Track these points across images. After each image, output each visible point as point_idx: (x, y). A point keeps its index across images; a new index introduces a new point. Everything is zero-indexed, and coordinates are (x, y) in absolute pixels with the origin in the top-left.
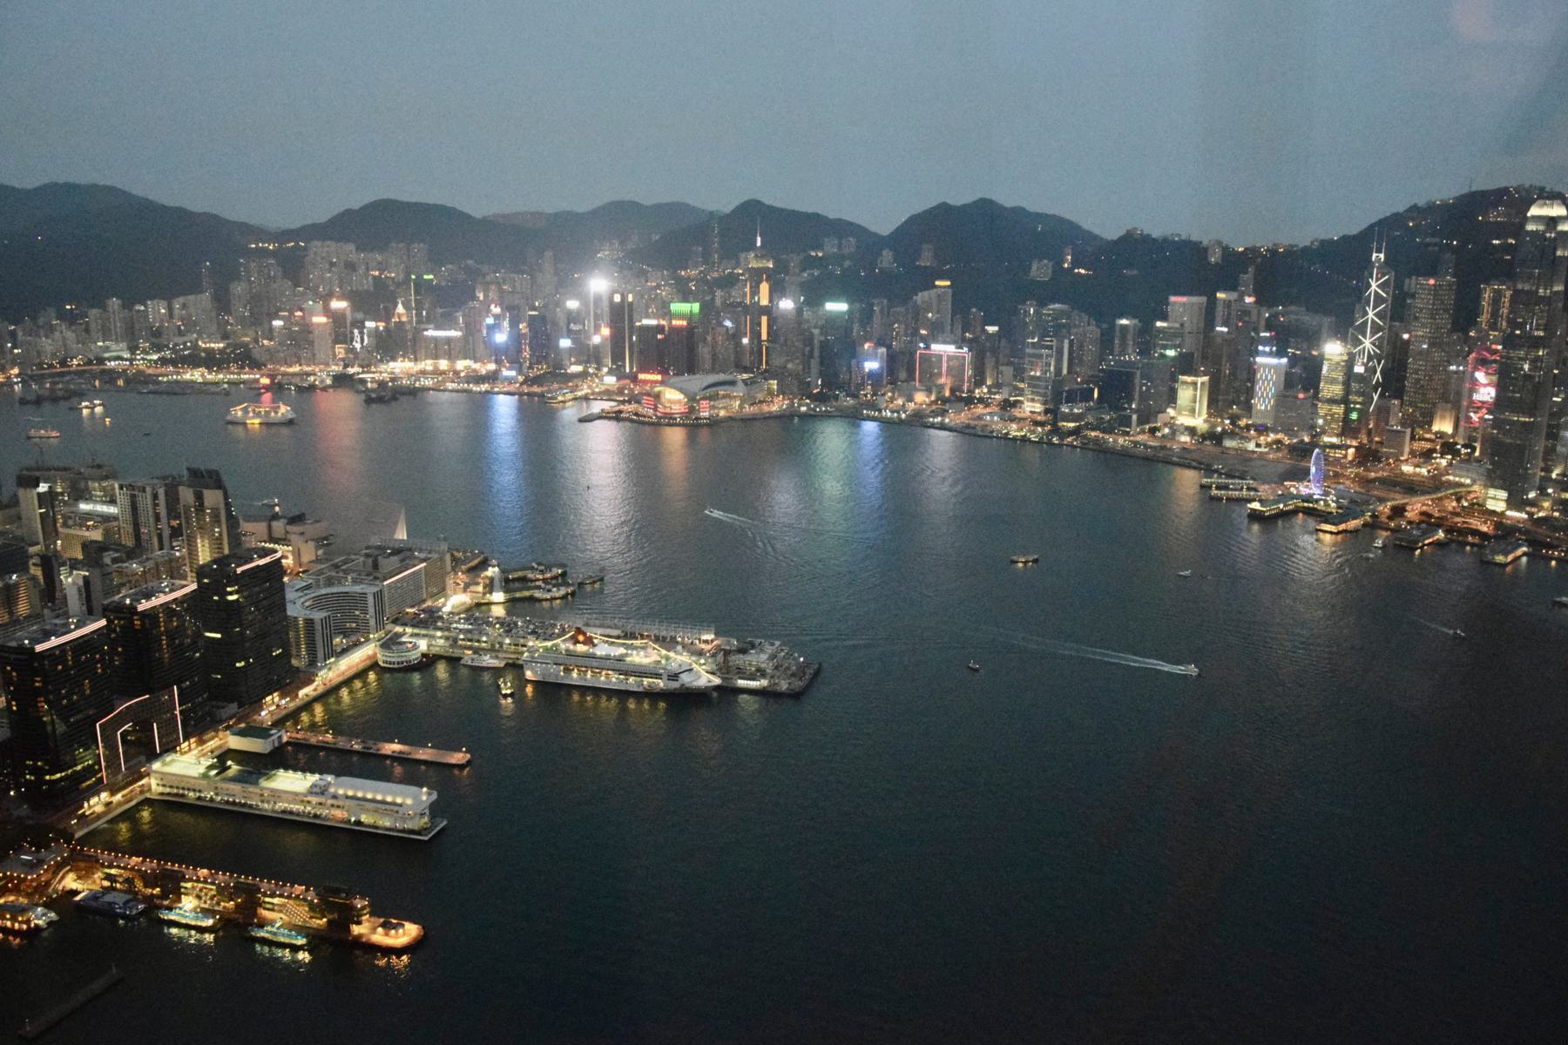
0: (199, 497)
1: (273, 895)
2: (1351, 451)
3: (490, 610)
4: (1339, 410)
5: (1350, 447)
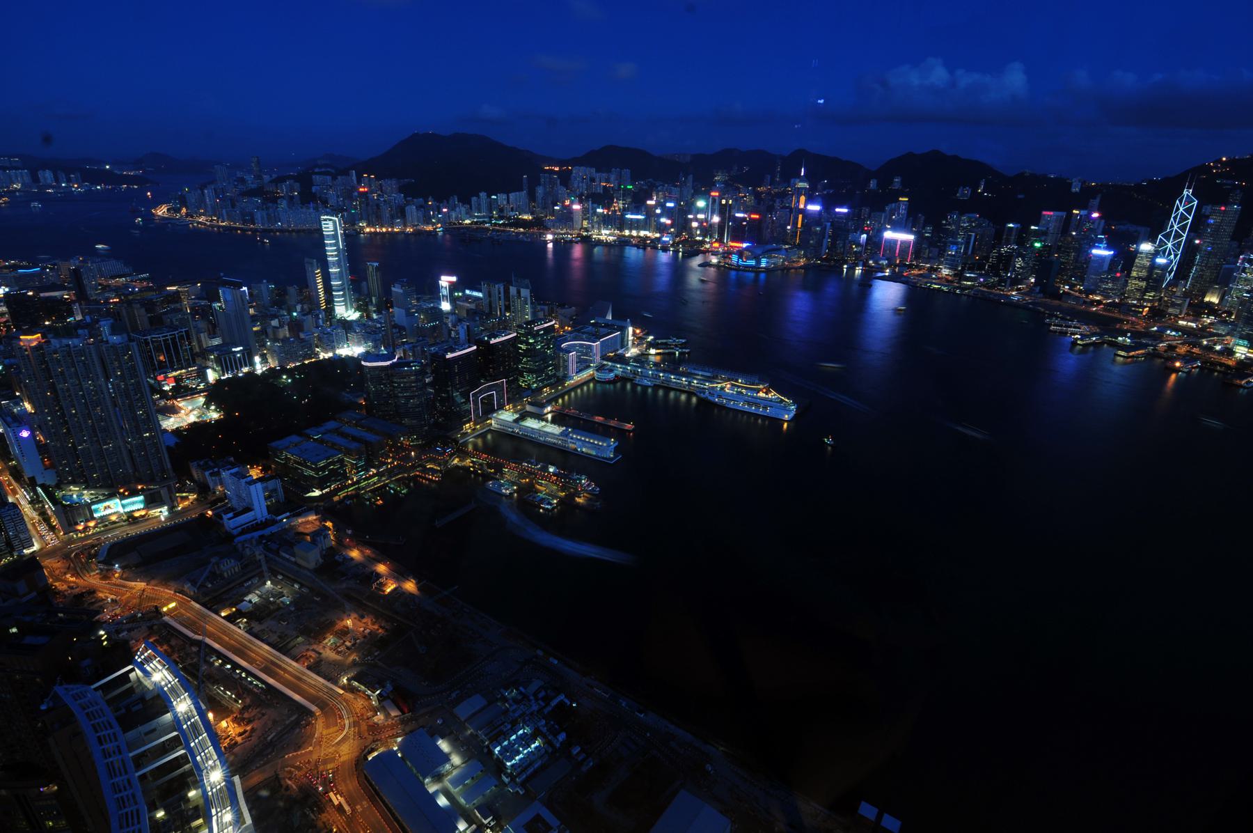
0: (519, 292)
1: (542, 480)
2: (1147, 309)
3: (648, 359)
4: (1144, 284)
5: (1146, 307)
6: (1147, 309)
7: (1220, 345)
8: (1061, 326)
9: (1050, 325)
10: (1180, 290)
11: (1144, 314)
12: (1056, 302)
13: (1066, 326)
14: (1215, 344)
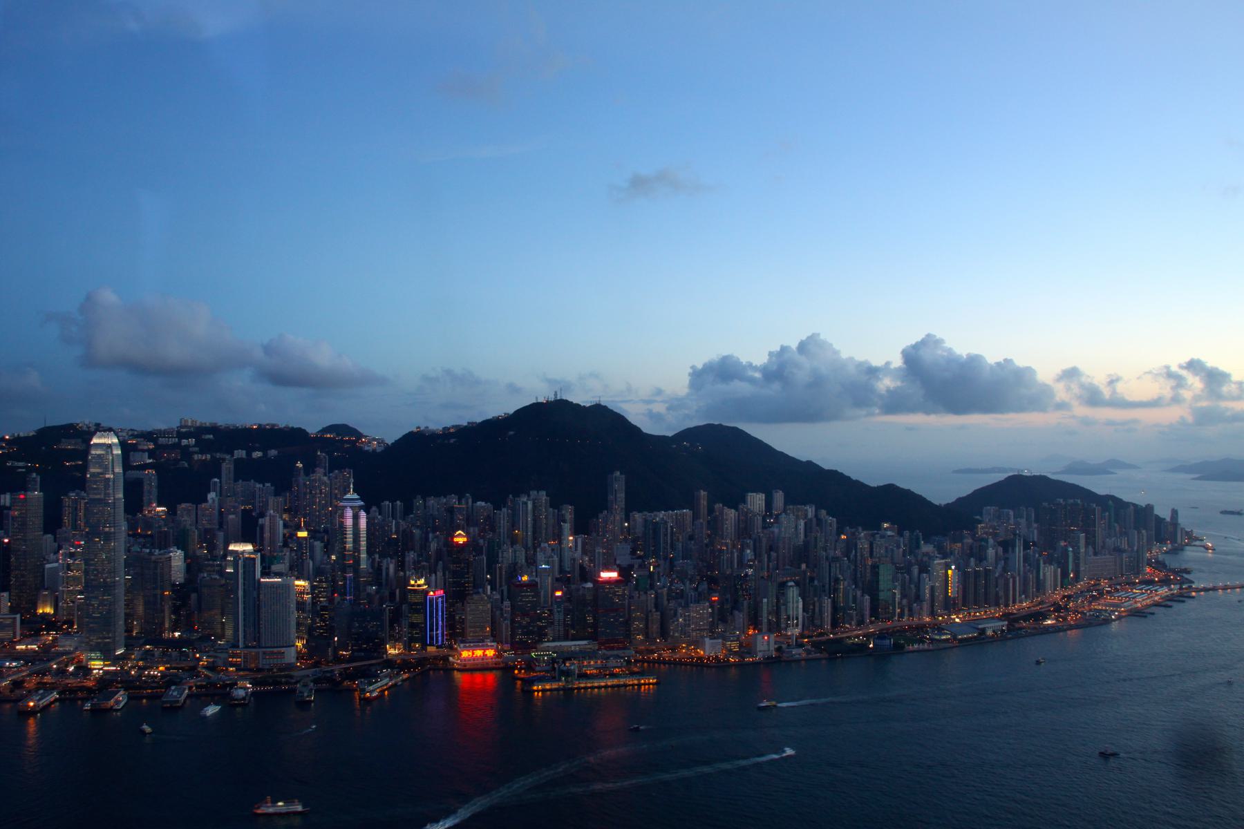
7: (72, 664)
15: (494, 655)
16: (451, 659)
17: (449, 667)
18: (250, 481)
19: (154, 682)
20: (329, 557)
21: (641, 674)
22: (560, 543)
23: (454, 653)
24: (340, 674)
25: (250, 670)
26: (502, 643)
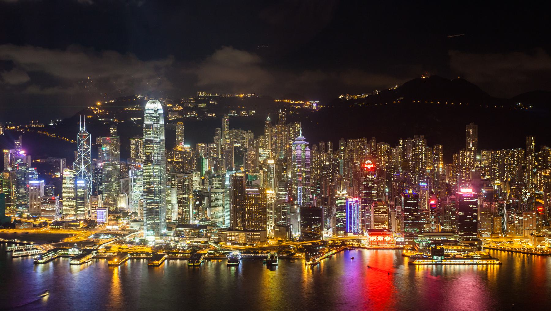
2: (82, 222)
4: (74, 202)
6: (82, 222)
8: (21, 250)
9: (12, 251)
10: (100, 202)
11: (81, 226)
12: (11, 231)
13: (26, 250)
14: (134, 238)
15: (390, 240)
16: (362, 241)
17: (361, 246)
18: (239, 129)
19: (183, 250)
20: (287, 177)
21: (489, 257)
22: (433, 170)
23: (365, 238)
24: (294, 248)
25: (240, 244)
26: (395, 232)
